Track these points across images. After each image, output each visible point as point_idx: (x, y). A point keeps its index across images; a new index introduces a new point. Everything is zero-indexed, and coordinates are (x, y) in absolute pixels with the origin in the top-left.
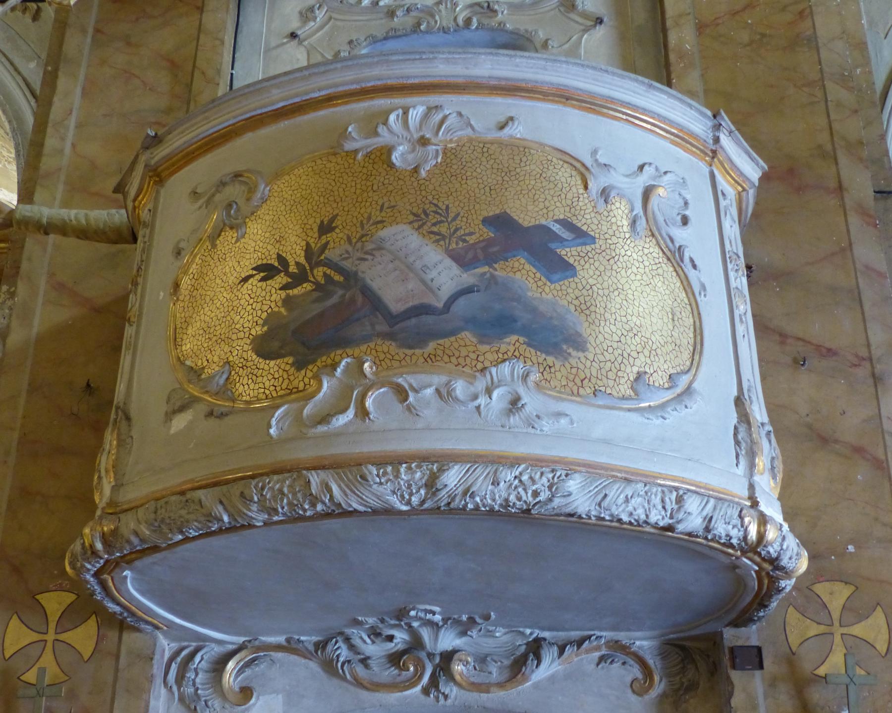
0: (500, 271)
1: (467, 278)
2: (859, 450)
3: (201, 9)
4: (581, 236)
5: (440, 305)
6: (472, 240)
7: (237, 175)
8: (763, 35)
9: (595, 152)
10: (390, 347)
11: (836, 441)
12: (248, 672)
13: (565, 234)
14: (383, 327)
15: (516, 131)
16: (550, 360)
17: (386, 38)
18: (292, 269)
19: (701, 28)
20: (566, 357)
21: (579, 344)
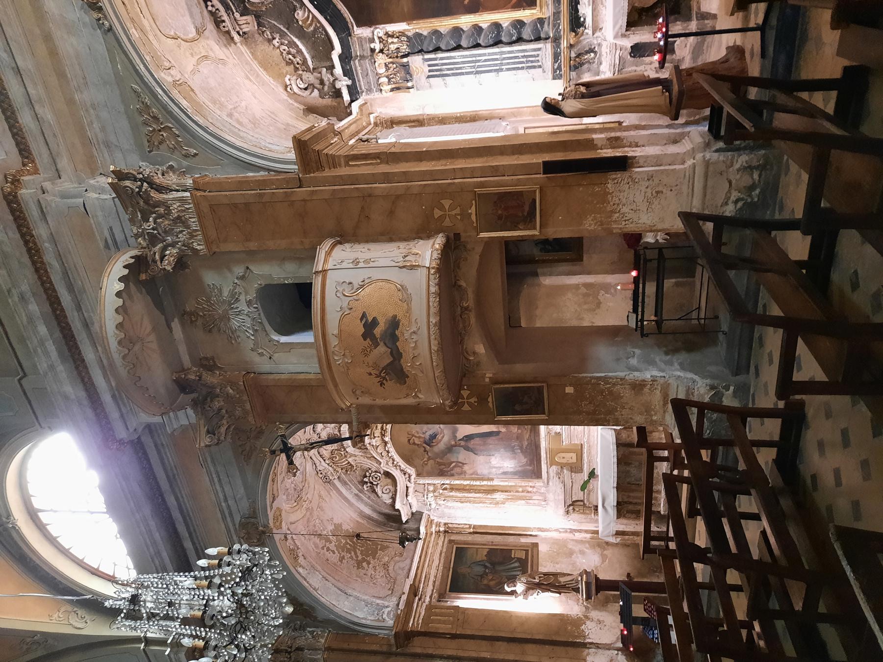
0: (378, 336)
1: (382, 344)
2: (393, 203)
3: (267, 386)
4: (364, 315)
5: (390, 350)
6: (371, 343)
7: (353, 393)
8: (247, 220)
9: (338, 311)
10: (402, 361)
11: (391, 209)
12: (469, 353)
13: (364, 320)
14: (397, 362)
15: (336, 332)
16: (401, 324)
17: (266, 331)
18: (382, 380)
19: (248, 240)
20: (399, 320)
21: (395, 317)
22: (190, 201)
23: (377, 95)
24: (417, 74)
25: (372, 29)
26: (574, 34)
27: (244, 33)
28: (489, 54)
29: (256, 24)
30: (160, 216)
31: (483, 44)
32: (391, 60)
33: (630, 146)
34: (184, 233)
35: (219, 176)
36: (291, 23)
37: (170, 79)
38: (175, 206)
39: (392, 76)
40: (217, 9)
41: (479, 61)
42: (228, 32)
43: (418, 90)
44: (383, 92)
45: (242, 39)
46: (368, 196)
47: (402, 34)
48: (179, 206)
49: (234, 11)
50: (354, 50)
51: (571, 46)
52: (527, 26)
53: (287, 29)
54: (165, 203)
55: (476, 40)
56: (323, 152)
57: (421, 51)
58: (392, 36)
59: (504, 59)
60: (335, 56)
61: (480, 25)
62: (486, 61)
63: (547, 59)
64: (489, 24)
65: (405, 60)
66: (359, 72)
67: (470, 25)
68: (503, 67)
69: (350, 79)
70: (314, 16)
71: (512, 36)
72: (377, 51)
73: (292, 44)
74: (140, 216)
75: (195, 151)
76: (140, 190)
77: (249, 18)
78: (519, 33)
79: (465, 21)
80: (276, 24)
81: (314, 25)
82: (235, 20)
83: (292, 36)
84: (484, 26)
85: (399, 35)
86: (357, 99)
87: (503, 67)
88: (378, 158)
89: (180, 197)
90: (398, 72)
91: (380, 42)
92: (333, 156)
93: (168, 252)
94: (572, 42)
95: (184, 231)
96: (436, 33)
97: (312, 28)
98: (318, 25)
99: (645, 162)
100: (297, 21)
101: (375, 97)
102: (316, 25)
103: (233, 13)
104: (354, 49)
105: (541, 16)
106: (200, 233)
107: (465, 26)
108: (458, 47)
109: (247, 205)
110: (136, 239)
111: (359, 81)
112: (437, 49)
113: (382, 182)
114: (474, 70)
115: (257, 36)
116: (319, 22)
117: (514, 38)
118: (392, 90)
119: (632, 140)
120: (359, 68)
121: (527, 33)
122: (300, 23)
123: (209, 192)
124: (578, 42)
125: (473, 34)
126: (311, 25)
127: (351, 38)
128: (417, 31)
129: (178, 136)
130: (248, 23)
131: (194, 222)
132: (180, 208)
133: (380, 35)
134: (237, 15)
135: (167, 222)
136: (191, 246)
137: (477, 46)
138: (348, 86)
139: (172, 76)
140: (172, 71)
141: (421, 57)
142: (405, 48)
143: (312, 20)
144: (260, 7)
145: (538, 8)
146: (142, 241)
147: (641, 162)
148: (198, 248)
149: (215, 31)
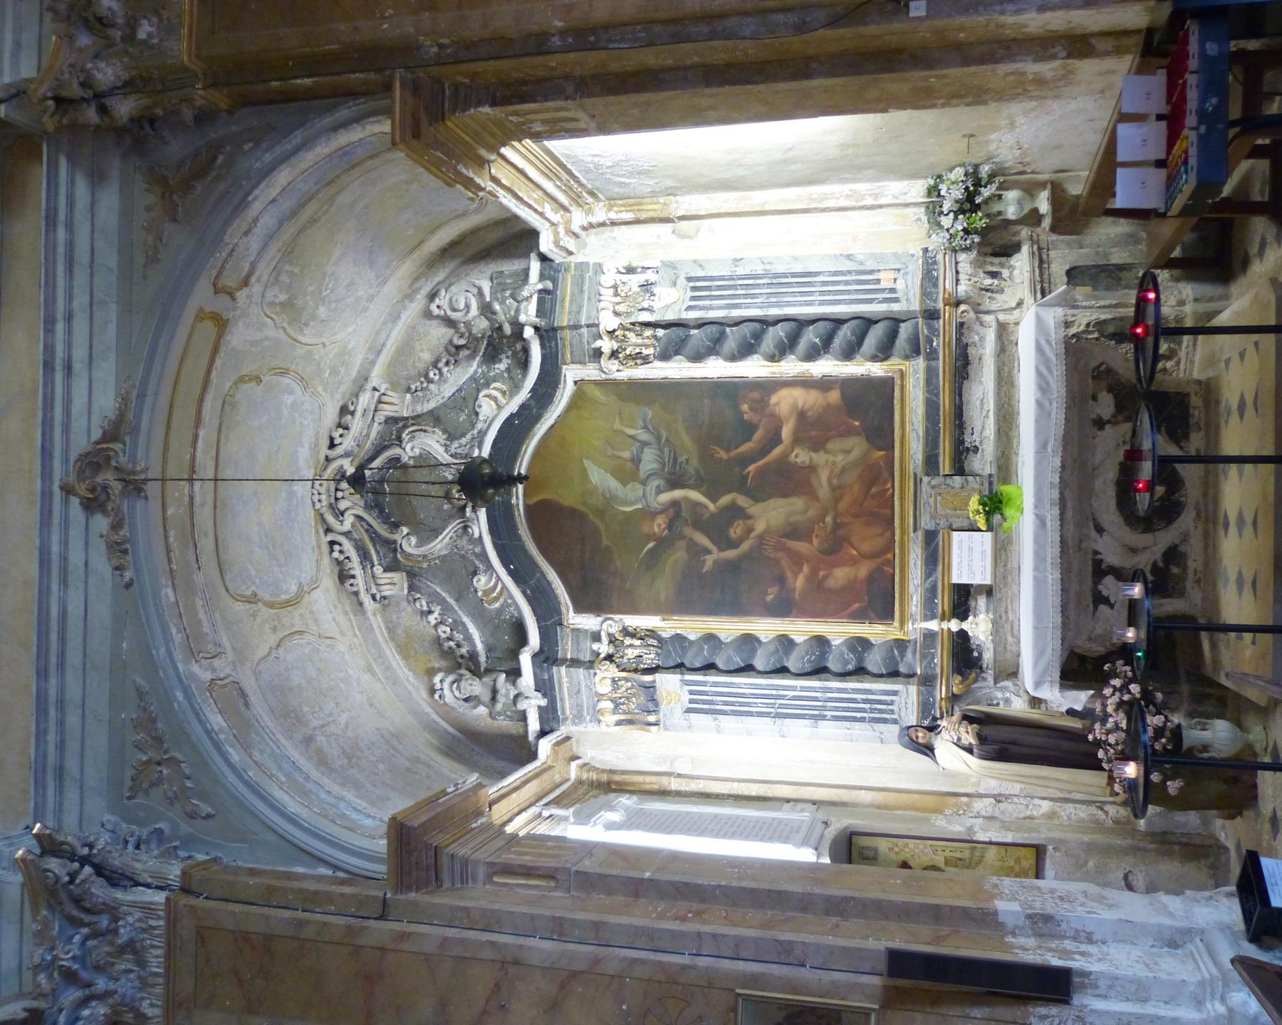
22: (161, 913)
23: (591, 728)
24: (669, 704)
25: (600, 619)
26: (960, 678)
27: (384, 598)
28: (803, 689)
29: (406, 585)
30: (95, 935)
31: (792, 669)
32: (624, 674)
33: (1075, 939)
34: (132, 976)
35: (240, 864)
36: (463, 591)
37: (208, 676)
38: (130, 919)
39: (622, 700)
40: (348, 558)
41: (782, 697)
42: (356, 594)
43: (666, 729)
44: (603, 724)
45: (377, 605)
46: (511, 964)
47: (652, 633)
48: (140, 920)
49: (376, 562)
50: (563, 648)
51: (954, 699)
52: (875, 650)
53: (457, 600)
54: (115, 908)
55: (781, 660)
56: (447, 850)
57: (680, 667)
58: (633, 636)
59: (830, 700)
60: (525, 659)
61: (792, 637)
62: (794, 698)
63: (910, 710)
64: (806, 638)
65: (648, 678)
66: (565, 686)
67: (772, 635)
68: (826, 713)
69: (545, 695)
70: (504, 587)
71: (847, 662)
72: (602, 656)
73: (457, 625)
74: (57, 928)
75: (210, 810)
76: (71, 882)
77: (396, 576)
78: (860, 659)
79: (766, 628)
80: (439, 590)
81: (502, 600)
82: (373, 577)
83: (460, 612)
84: (799, 639)
86: (552, 731)
87: (826, 713)
88: (552, 877)
89: (146, 903)
90: (634, 695)
91: (611, 642)
92: (465, 862)
93: (86, 1012)
94: (955, 690)
95: (130, 971)
96: (711, 638)
97: (497, 605)
98: (509, 601)
99: (1110, 987)
100: (476, 591)
101: (587, 729)
102: (505, 601)
103: (373, 566)
104: (563, 648)
105: (900, 636)
106: (161, 980)
108: (748, 669)
109: (268, 939)
110: (35, 975)
111: (562, 700)
112: (710, 667)
113: (548, 935)
114: (772, 710)
115: (404, 604)
116: (511, 597)
117: (850, 667)
118: (619, 723)
119: (1080, 927)
120: (565, 680)
121: (874, 661)
122: (480, 594)
123: (206, 898)
124: (968, 691)
125: (777, 651)
126: (497, 599)
129: (188, 778)
130: (395, 584)
131: (157, 957)
132: (138, 925)
133: (612, 631)
134: (378, 570)
135: (107, 949)
136: (137, 1004)
137: (782, 671)
138: (540, 707)
139: (214, 670)
140: (217, 663)
141: (678, 677)
142: (650, 658)
143: (500, 594)
144: (419, 562)
145: (896, 624)
146: (44, 981)
147: (1103, 984)
148: (150, 1012)
149: (333, 590)
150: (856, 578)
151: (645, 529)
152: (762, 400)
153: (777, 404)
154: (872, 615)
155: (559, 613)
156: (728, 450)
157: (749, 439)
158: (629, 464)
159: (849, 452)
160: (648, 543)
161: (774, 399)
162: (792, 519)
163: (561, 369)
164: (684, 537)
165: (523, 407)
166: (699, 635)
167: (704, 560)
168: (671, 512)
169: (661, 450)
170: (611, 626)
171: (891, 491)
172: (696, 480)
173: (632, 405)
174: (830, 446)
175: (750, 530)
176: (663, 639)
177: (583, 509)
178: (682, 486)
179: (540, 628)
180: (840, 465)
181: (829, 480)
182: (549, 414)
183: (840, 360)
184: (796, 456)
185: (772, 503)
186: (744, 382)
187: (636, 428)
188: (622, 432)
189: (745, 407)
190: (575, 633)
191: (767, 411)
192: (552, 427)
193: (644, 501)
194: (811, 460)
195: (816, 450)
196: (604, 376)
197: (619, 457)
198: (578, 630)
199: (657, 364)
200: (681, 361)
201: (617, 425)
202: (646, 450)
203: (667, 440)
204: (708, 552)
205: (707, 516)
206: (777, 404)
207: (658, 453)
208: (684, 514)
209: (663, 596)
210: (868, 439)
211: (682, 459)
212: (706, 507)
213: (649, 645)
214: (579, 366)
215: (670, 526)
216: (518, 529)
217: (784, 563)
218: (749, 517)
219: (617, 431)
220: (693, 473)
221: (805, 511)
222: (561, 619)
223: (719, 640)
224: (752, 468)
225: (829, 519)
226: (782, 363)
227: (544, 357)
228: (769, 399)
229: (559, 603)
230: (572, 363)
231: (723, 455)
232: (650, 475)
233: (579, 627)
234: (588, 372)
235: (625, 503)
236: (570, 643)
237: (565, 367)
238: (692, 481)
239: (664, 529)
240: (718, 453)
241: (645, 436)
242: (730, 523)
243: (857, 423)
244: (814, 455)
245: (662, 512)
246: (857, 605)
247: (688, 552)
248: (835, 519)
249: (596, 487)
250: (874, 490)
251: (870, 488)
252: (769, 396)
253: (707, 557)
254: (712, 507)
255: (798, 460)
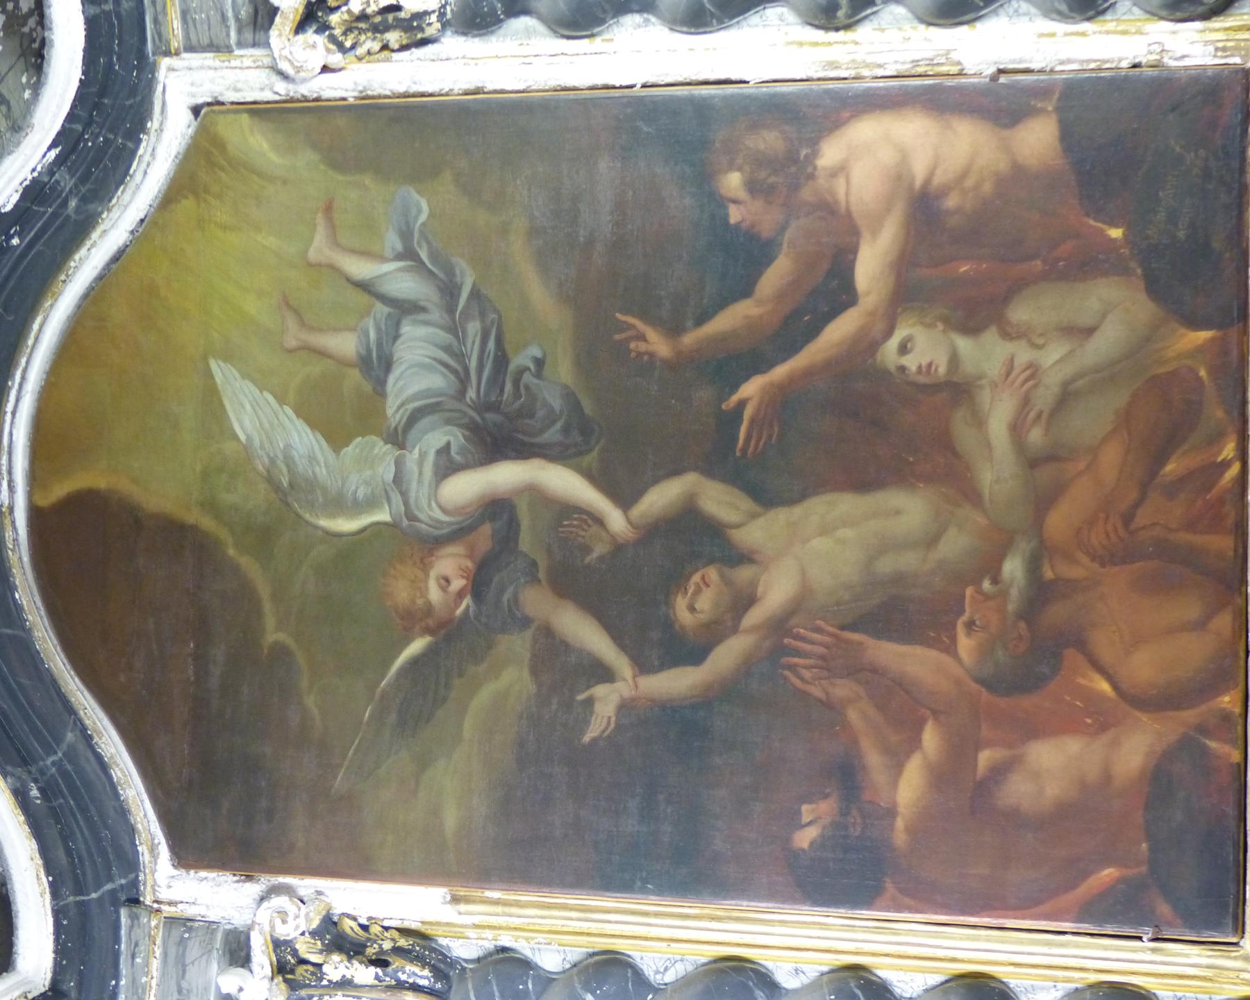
25: (253, 889)
50: (134, 981)
61: (883, 974)
67: (816, 966)
85: (397, 951)
91: (281, 969)
104: (134, 981)
107: (789, 967)
127: (134, 918)
128: (506, 940)
133: (285, 931)
150: (1107, 778)
151: (401, 593)
152: (791, 158)
153: (841, 170)
154: (1164, 909)
155: (131, 864)
156: (674, 330)
157: (746, 291)
158: (355, 375)
159: (1090, 331)
160: (407, 641)
161: (831, 153)
162: (887, 565)
163: (153, 68)
164: (526, 622)
165: (35, 193)
166: (575, 955)
167: (590, 702)
168: (484, 537)
169: (455, 329)
170: (283, 915)
171: (1235, 469)
172: (566, 430)
173: (367, 180)
174: (1021, 313)
175: (745, 600)
176: (452, 963)
177: (207, 523)
178: (522, 450)
179: (58, 913)
180: (1052, 382)
181: (1017, 429)
182: (115, 214)
183: (1063, 17)
184: (904, 349)
185: (818, 508)
186: (726, 98)
187: (382, 259)
188: (333, 269)
189: (733, 182)
190: (177, 932)
191: (806, 194)
192: (117, 257)
193: (396, 498)
194: (954, 360)
195: (971, 328)
196: (282, 88)
197: (322, 353)
198: (186, 922)
199: (453, 44)
200: (529, 33)
201: (319, 248)
202: (407, 329)
203: (475, 294)
204: (605, 674)
205: (600, 550)
206: (841, 170)
207: (446, 337)
208: (526, 542)
209: (451, 819)
210: (1154, 288)
211: (522, 359)
212: (598, 520)
213: (401, 986)
214: (208, 59)
215: (479, 584)
216: (12, 588)
217: (853, 715)
218: (739, 557)
219: (318, 266)
220: (557, 403)
221: (932, 541)
222: (135, 884)
223: (638, 975)
224: (751, 389)
225: (1013, 568)
226: (864, 32)
227: (92, 26)
228: (815, 154)
229: (132, 831)
230: (190, 48)
231: (658, 344)
232: (414, 418)
233: (190, 911)
234: (230, 76)
235: (339, 504)
236: (155, 964)
237: (165, 62)
238: (552, 435)
239: (460, 595)
240: (642, 337)
241: (405, 285)
242: (675, 579)
243: (1116, 233)
244: (964, 344)
245: (458, 534)
246: (1109, 873)
247: (535, 672)
248: (1034, 565)
249: (247, 448)
250: (1171, 468)
251: (1161, 458)
252: (814, 144)
253: (600, 690)
254: (616, 520)
255: (911, 362)
